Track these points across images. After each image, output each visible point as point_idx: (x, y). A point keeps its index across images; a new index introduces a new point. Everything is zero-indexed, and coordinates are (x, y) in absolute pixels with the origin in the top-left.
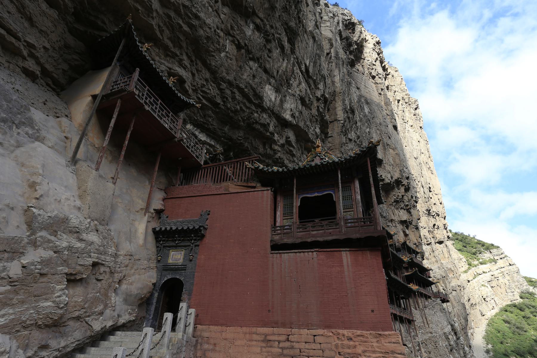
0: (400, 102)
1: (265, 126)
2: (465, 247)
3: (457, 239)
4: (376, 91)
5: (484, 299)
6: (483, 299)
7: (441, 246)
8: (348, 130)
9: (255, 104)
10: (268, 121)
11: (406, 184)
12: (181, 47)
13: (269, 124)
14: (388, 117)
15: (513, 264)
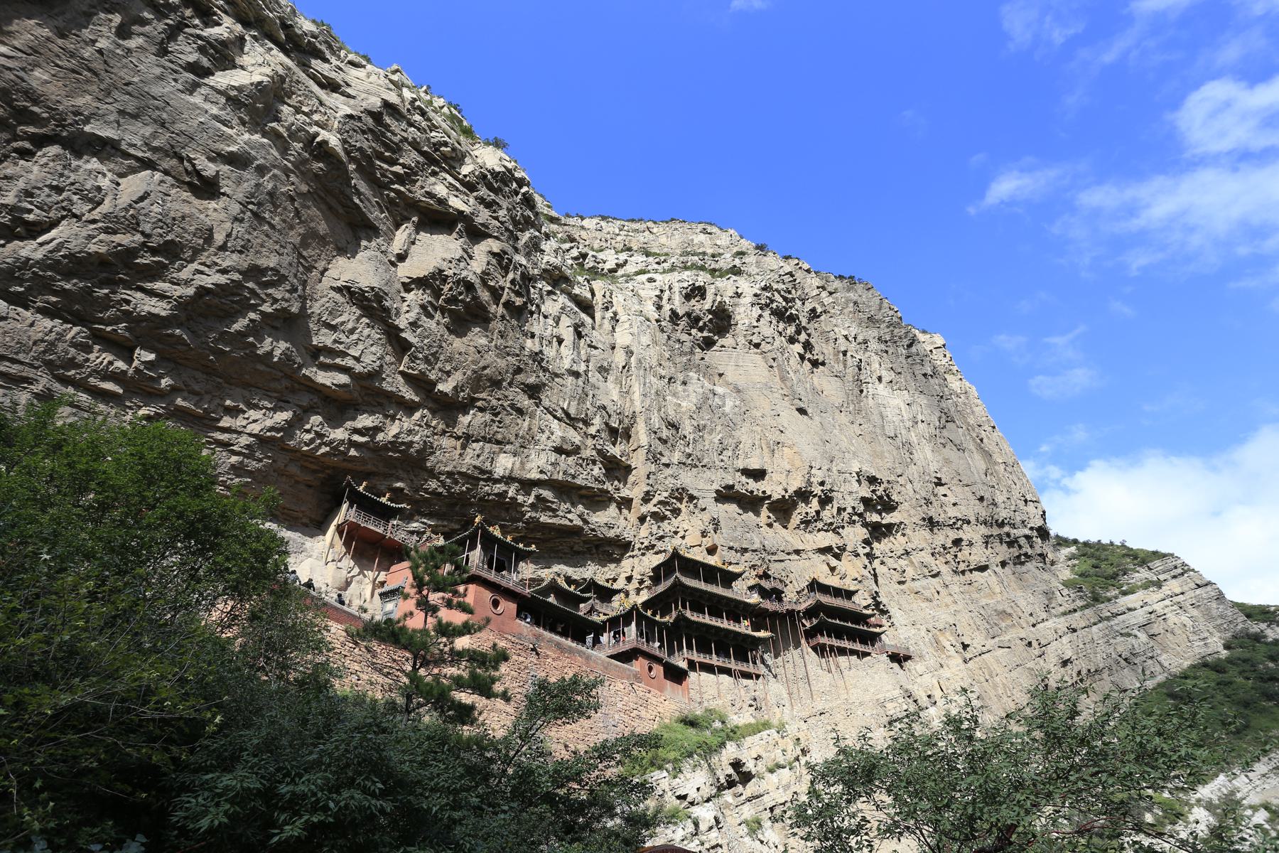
0: (849, 354)
1: (503, 495)
2: (1096, 567)
3: (1084, 555)
4: (764, 363)
5: (1126, 660)
6: (1123, 662)
7: (986, 573)
8: (661, 454)
9: (483, 480)
10: (504, 488)
11: (820, 493)
12: (396, 467)
13: (506, 492)
14: (786, 398)
15: (1204, 582)
